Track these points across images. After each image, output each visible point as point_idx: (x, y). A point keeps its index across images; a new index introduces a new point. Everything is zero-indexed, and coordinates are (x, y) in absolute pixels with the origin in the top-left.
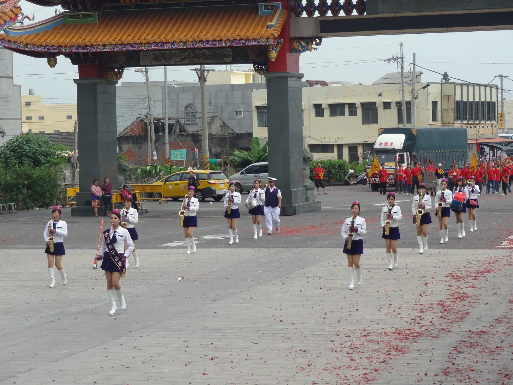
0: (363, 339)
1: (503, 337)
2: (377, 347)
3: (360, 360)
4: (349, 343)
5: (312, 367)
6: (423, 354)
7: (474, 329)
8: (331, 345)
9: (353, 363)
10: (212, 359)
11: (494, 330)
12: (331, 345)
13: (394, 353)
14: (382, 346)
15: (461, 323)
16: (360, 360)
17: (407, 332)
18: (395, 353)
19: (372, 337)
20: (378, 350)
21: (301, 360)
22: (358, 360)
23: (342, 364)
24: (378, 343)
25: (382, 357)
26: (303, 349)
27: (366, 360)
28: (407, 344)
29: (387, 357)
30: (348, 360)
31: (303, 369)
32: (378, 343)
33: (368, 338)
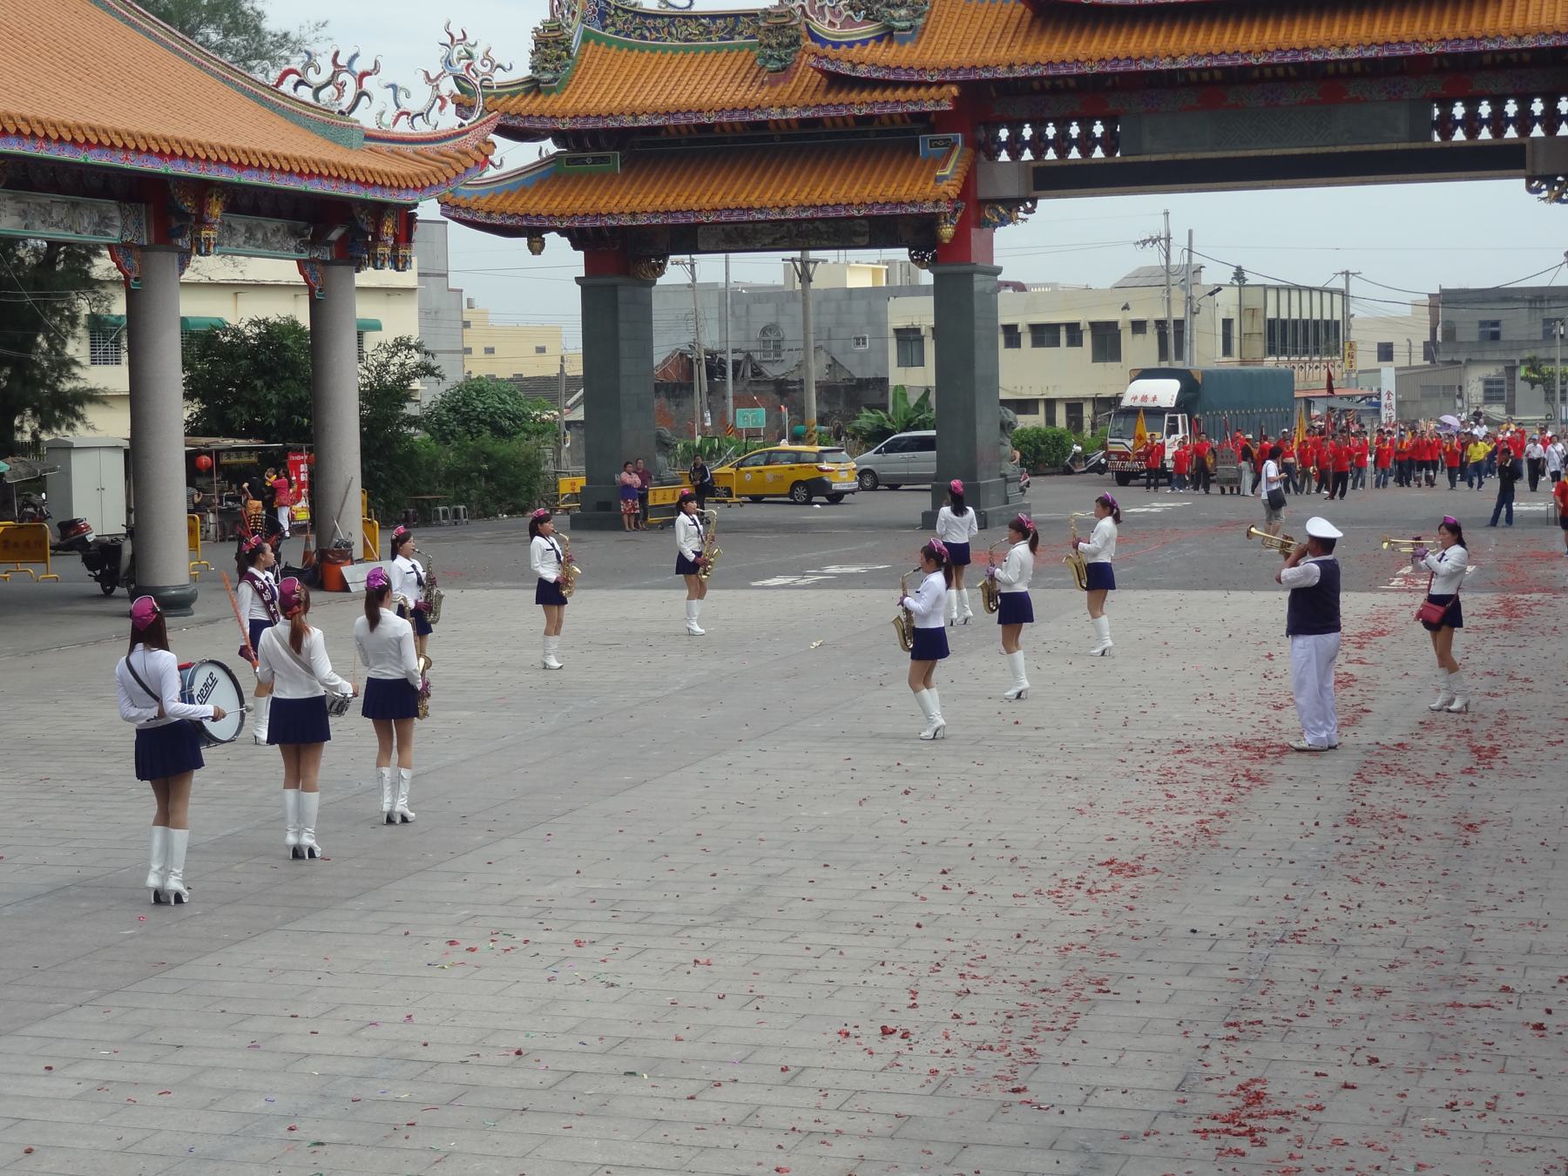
0: (1180, 757)
1: (1444, 755)
2: (1208, 772)
3: (1184, 797)
4: (1156, 766)
5: (1097, 808)
6: (1301, 787)
7: (1384, 740)
8: (1123, 769)
9: (1172, 803)
10: (907, 793)
11: (1421, 742)
12: (1123, 769)
13: (1244, 783)
14: (1218, 770)
15: (1355, 729)
16: (1184, 797)
17: (1258, 744)
18: (1247, 784)
19: (1196, 754)
20: (1214, 779)
21: (1072, 796)
22: (1181, 797)
23: (1152, 804)
24: (1210, 764)
25: (1226, 790)
26: (1073, 775)
27: (1195, 797)
28: (1265, 766)
29: (1232, 790)
30: (1162, 796)
31: (1081, 812)
32: (1210, 764)
33: (1188, 756)
